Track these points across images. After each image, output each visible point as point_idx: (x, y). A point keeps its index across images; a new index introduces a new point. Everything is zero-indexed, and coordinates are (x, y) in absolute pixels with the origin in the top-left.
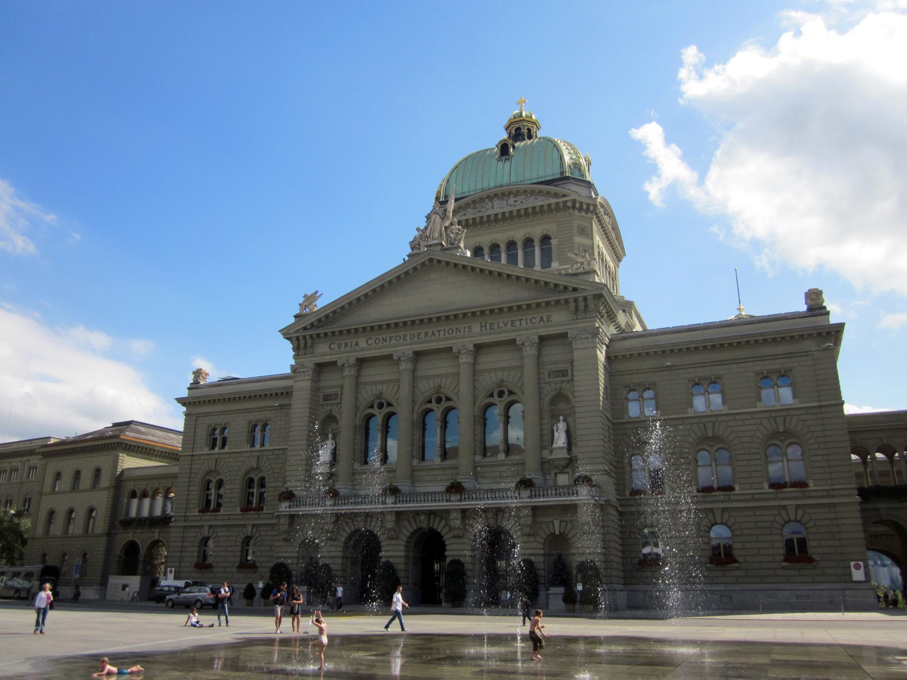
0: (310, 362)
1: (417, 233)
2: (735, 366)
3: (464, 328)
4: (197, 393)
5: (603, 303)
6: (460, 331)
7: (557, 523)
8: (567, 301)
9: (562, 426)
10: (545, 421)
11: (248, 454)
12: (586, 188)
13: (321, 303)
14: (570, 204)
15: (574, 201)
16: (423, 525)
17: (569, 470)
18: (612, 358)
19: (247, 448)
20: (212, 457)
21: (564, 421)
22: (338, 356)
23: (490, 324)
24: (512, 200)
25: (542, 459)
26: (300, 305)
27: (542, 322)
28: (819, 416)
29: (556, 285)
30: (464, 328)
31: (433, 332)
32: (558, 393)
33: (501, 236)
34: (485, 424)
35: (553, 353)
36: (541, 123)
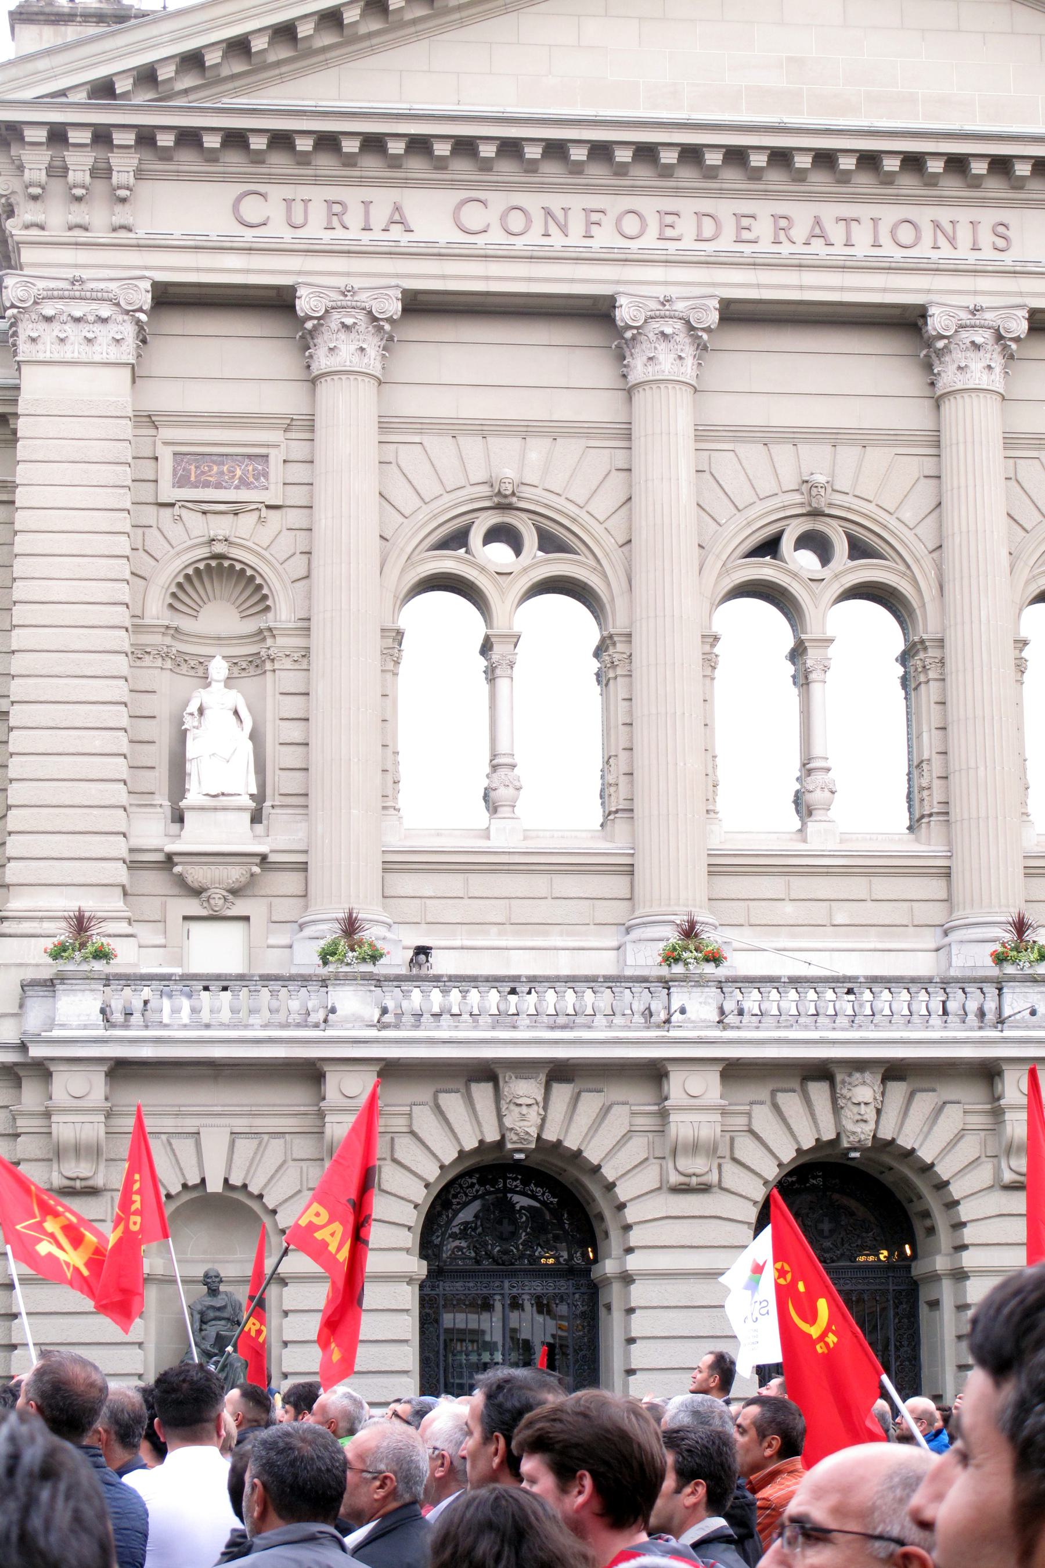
6: (952, 242)
22: (294, 263)
31: (818, 222)
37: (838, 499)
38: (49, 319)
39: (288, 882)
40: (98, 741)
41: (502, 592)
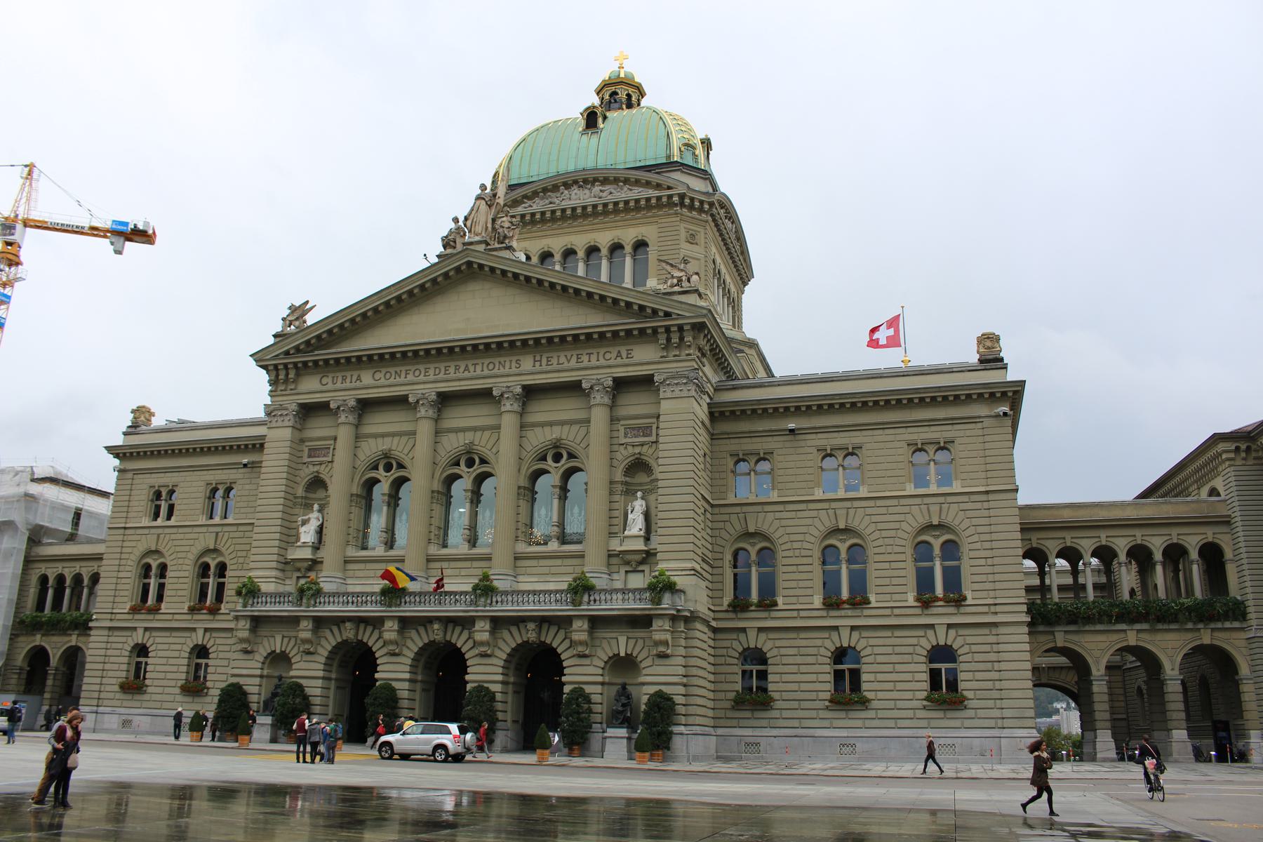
0: (291, 403)
1: (453, 225)
2: (880, 432)
3: (511, 361)
4: (135, 440)
5: (706, 336)
6: (504, 367)
7: (622, 640)
8: (655, 330)
9: (639, 505)
10: (616, 498)
11: (204, 529)
12: (701, 181)
13: (311, 319)
14: (676, 199)
15: (682, 196)
16: (436, 637)
17: (646, 568)
18: (717, 415)
19: (203, 520)
20: (153, 531)
21: (642, 498)
23: (548, 358)
24: (597, 189)
25: (609, 551)
26: (284, 319)
27: (619, 359)
28: (986, 505)
29: (642, 308)
30: (511, 361)
31: (467, 366)
32: (637, 459)
33: (580, 241)
34: (534, 500)
35: (634, 405)
36: (646, 88)
37: (475, 447)
38: (274, 416)
39: (319, 566)
40: (273, 529)
41: (387, 481)
